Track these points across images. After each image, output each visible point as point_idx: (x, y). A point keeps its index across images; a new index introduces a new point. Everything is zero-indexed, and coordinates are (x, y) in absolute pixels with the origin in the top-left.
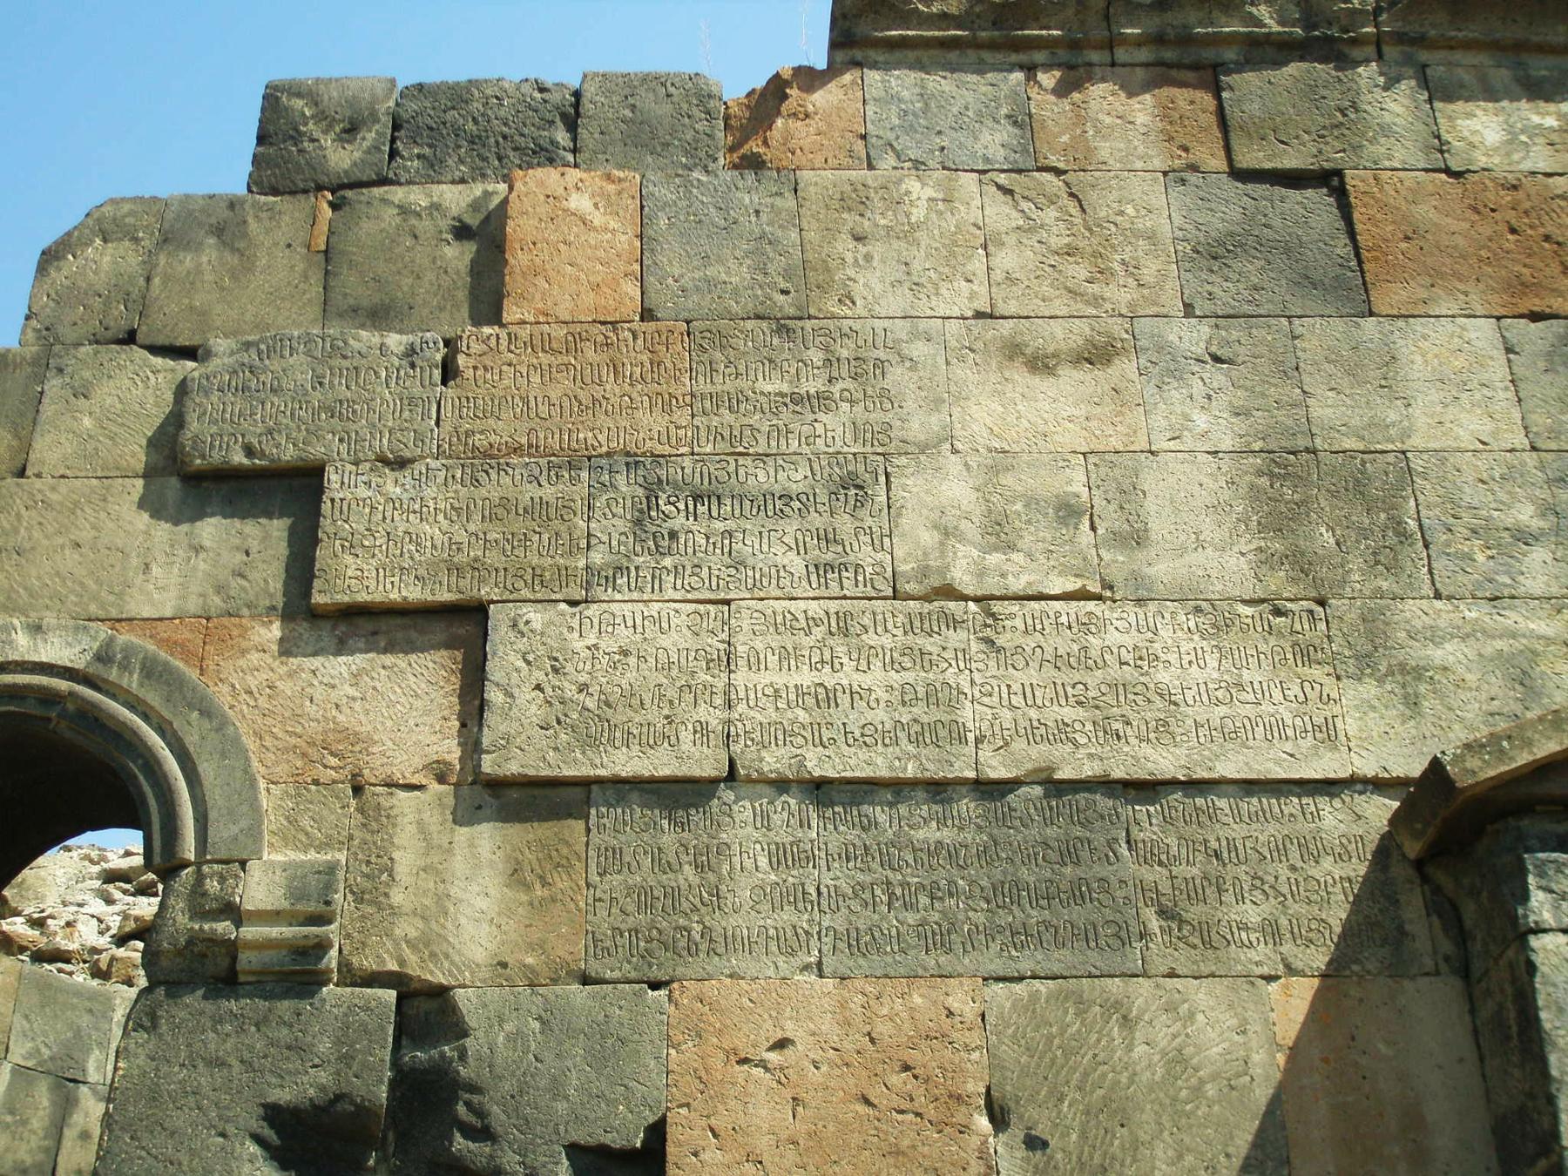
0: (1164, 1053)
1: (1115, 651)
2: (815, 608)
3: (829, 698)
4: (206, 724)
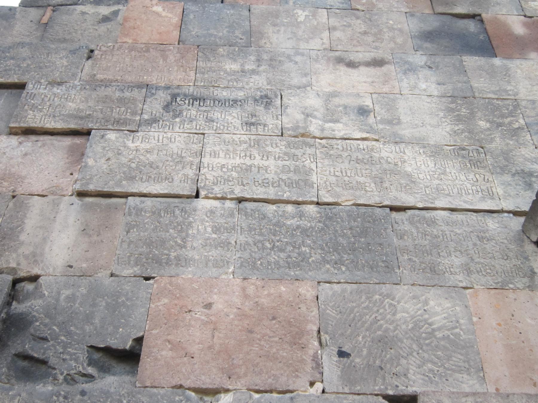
0: (413, 317)
1: (385, 158)
2: (244, 138)
3: (249, 169)
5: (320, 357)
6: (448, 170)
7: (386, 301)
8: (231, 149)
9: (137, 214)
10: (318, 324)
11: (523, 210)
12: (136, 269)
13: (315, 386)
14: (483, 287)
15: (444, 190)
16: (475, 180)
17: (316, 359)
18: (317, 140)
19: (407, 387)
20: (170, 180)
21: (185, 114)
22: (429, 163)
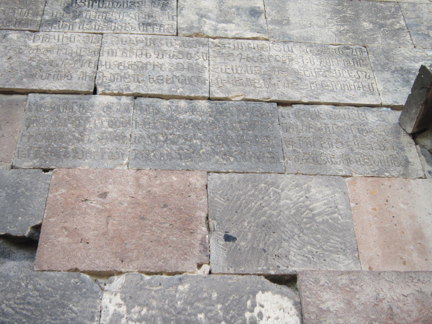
0: (295, 203)
1: (274, 56)
3: (144, 67)
5: (207, 241)
6: (332, 67)
7: (271, 189)
8: (128, 48)
9: (37, 110)
10: (207, 211)
11: (400, 104)
12: (35, 161)
13: (202, 267)
14: (361, 175)
15: (328, 86)
16: (357, 76)
17: (204, 243)
18: (210, 40)
19: (288, 267)
20: (69, 77)
21: (84, 15)
22: (315, 61)
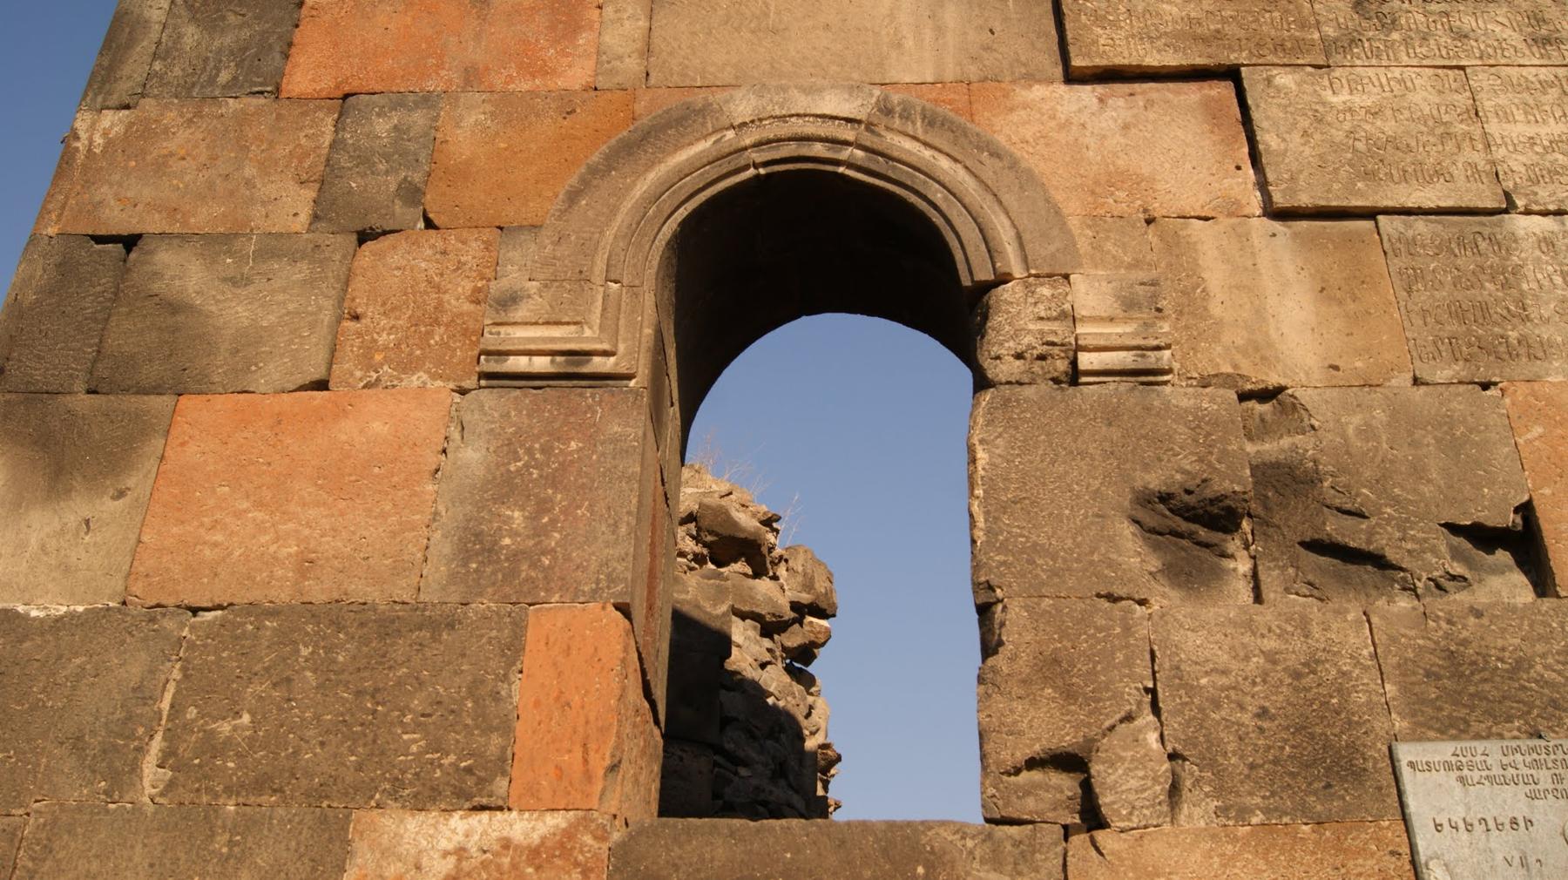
4: (998, 164)
21: (1403, 21)
